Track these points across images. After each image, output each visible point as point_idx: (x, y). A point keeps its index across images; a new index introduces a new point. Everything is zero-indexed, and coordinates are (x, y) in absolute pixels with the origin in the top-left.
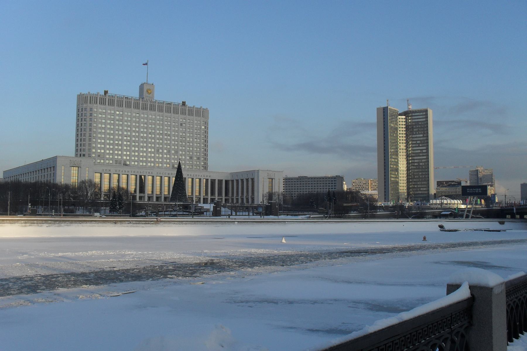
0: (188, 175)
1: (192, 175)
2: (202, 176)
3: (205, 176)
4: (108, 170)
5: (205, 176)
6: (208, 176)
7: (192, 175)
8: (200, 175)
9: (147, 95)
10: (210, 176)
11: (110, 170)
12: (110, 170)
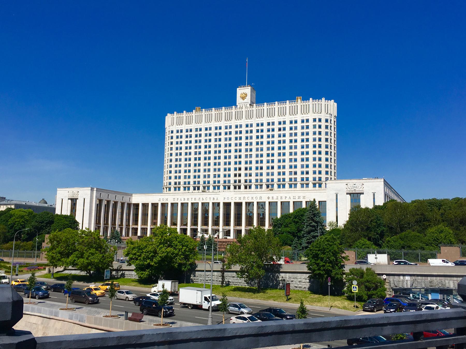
1: (275, 198)
2: (292, 198)
3: (297, 198)
4: (165, 199)
5: (297, 198)
7: (275, 198)
8: (288, 197)
10: (304, 197)
11: (167, 199)
12: (167, 199)
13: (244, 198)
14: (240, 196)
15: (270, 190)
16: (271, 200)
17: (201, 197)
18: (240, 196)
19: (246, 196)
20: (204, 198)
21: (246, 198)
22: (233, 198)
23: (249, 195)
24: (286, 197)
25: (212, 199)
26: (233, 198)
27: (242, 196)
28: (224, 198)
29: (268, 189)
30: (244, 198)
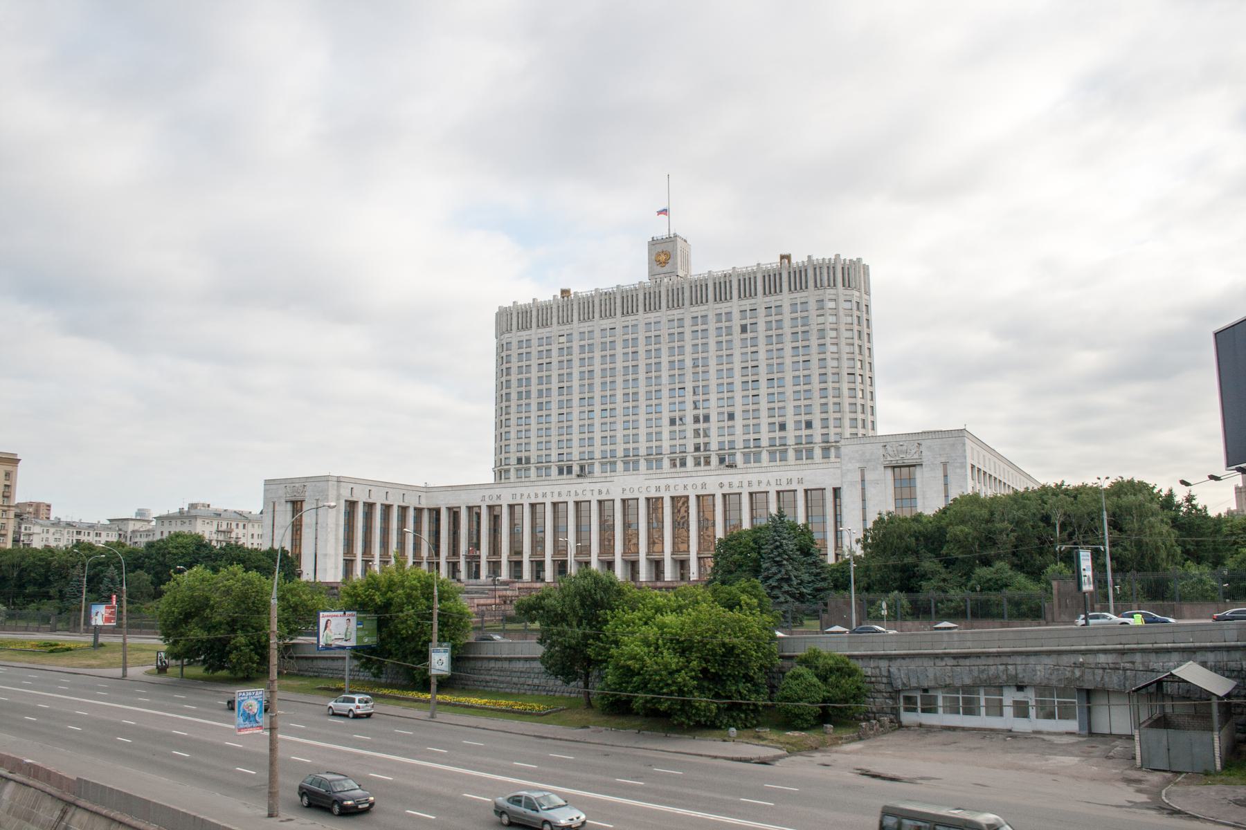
0: (721, 485)
1: (736, 483)
2: (773, 482)
3: (784, 481)
4: (495, 497)
6: (795, 481)
7: (736, 483)
8: (765, 481)
9: (659, 269)
10: (800, 481)
11: (499, 497)
12: (499, 497)
13: (667, 488)
14: (657, 483)
15: (730, 466)
16: (726, 490)
17: (573, 488)
18: (657, 483)
19: (670, 482)
20: (580, 492)
21: (672, 488)
22: (643, 490)
23: (678, 481)
24: (759, 482)
25: (596, 493)
26: (643, 490)
27: (662, 483)
28: (624, 490)
29: (722, 467)
30: (667, 488)
